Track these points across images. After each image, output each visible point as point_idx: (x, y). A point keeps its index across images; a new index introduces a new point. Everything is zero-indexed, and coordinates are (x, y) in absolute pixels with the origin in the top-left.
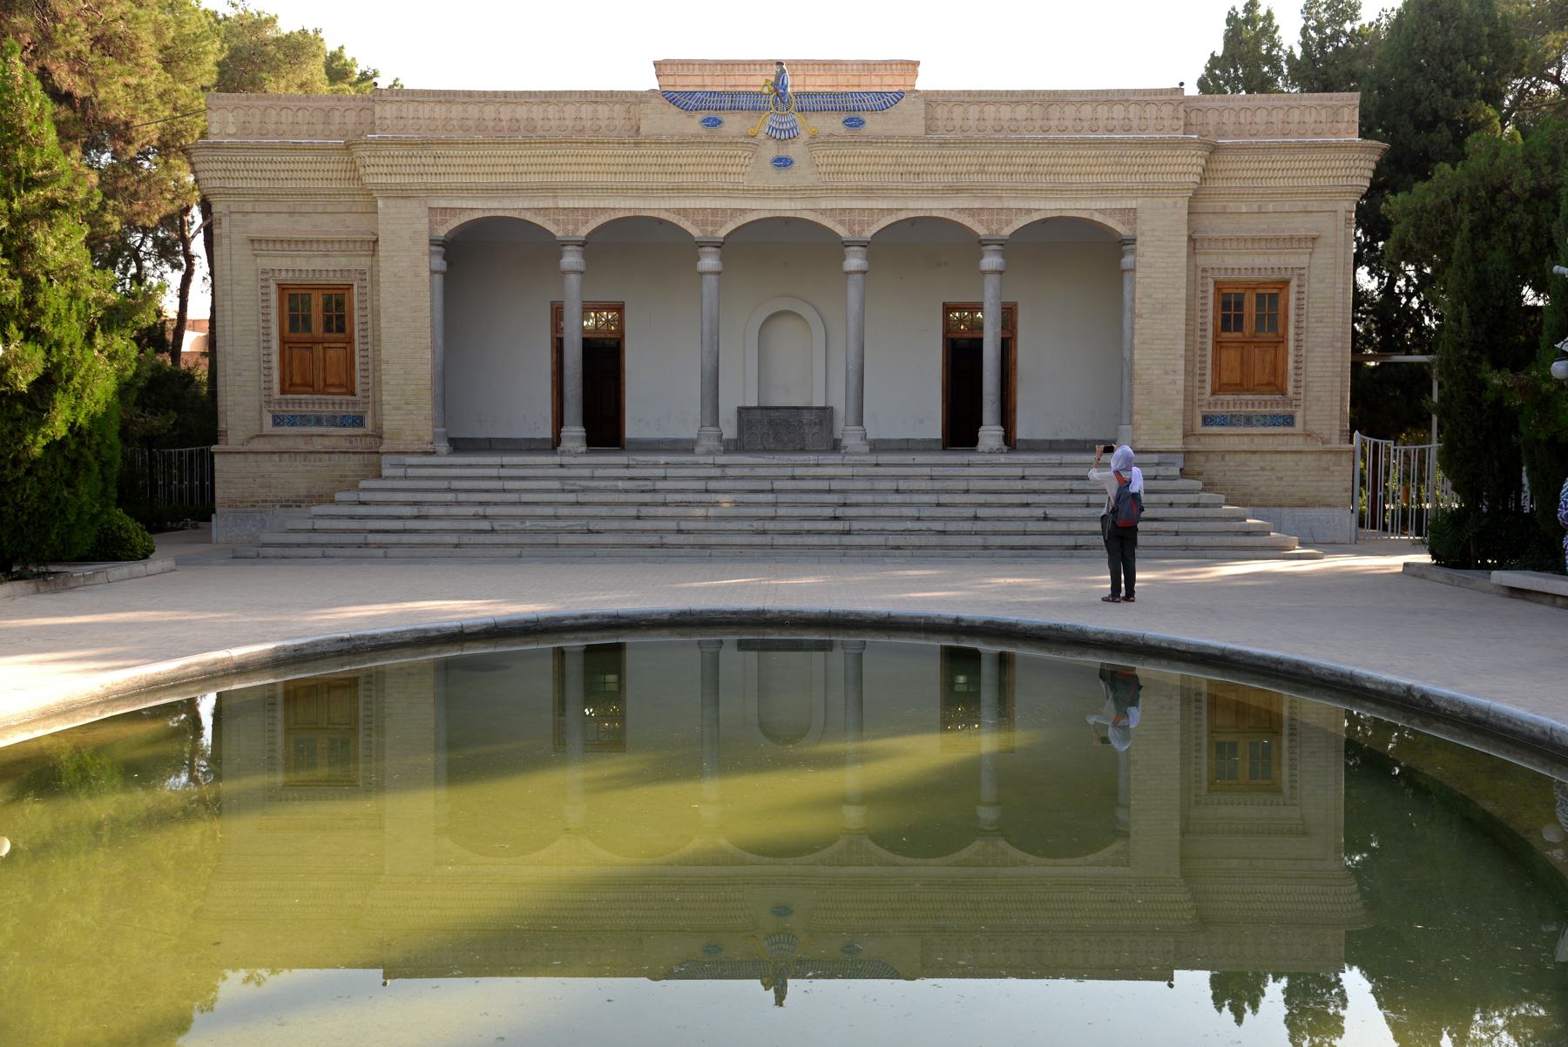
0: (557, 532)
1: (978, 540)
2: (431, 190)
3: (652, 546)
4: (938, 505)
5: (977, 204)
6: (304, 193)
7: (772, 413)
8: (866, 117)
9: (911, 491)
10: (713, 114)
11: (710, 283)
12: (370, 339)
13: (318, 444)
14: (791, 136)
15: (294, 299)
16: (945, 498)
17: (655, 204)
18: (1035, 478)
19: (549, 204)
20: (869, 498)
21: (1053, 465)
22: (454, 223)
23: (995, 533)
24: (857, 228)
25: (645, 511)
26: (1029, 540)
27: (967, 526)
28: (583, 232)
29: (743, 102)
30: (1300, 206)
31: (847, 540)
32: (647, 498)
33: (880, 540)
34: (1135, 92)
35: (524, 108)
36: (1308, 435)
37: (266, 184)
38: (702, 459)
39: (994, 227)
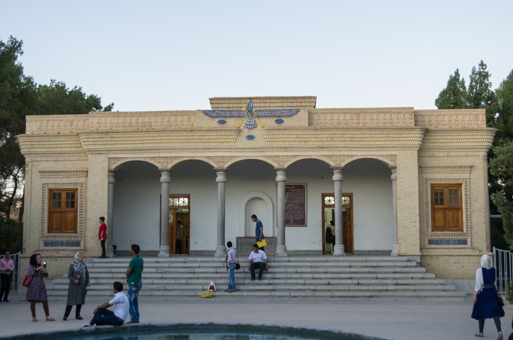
0: (152, 290)
1: (329, 294)
2: (109, 151)
3: (192, 296)
4: (314, 278)
5: (331, 153)
6: (60, 153)
7: (250, 240)
8: (284, 119)
9: (302, 273)
10: (223, 119)
11: (220, 186)
12: (84, 210)
13: (61, 254)
14: (254, 126)
15: (54, 195)
16: (316, 276)
17: (199, 155)
18: (355, 267)
19: (156, 155)
20: (284, 276)
21: (363, 261)
22: (119, 163)
23: (337, 290)
24: (281, 163)
25: (190, 281)
26: (350, 294)
27: (325, 287)
28: (170, 166)
29: (235, 113)
30: (464, 154)
31: (273, 293)
32: (191, 275)
33: (287, 294)
34: (394, 108)
35: (148, 118)
36: (473, 248)
37: (46, 150)
38: (215, 259)
39: (338, 162)
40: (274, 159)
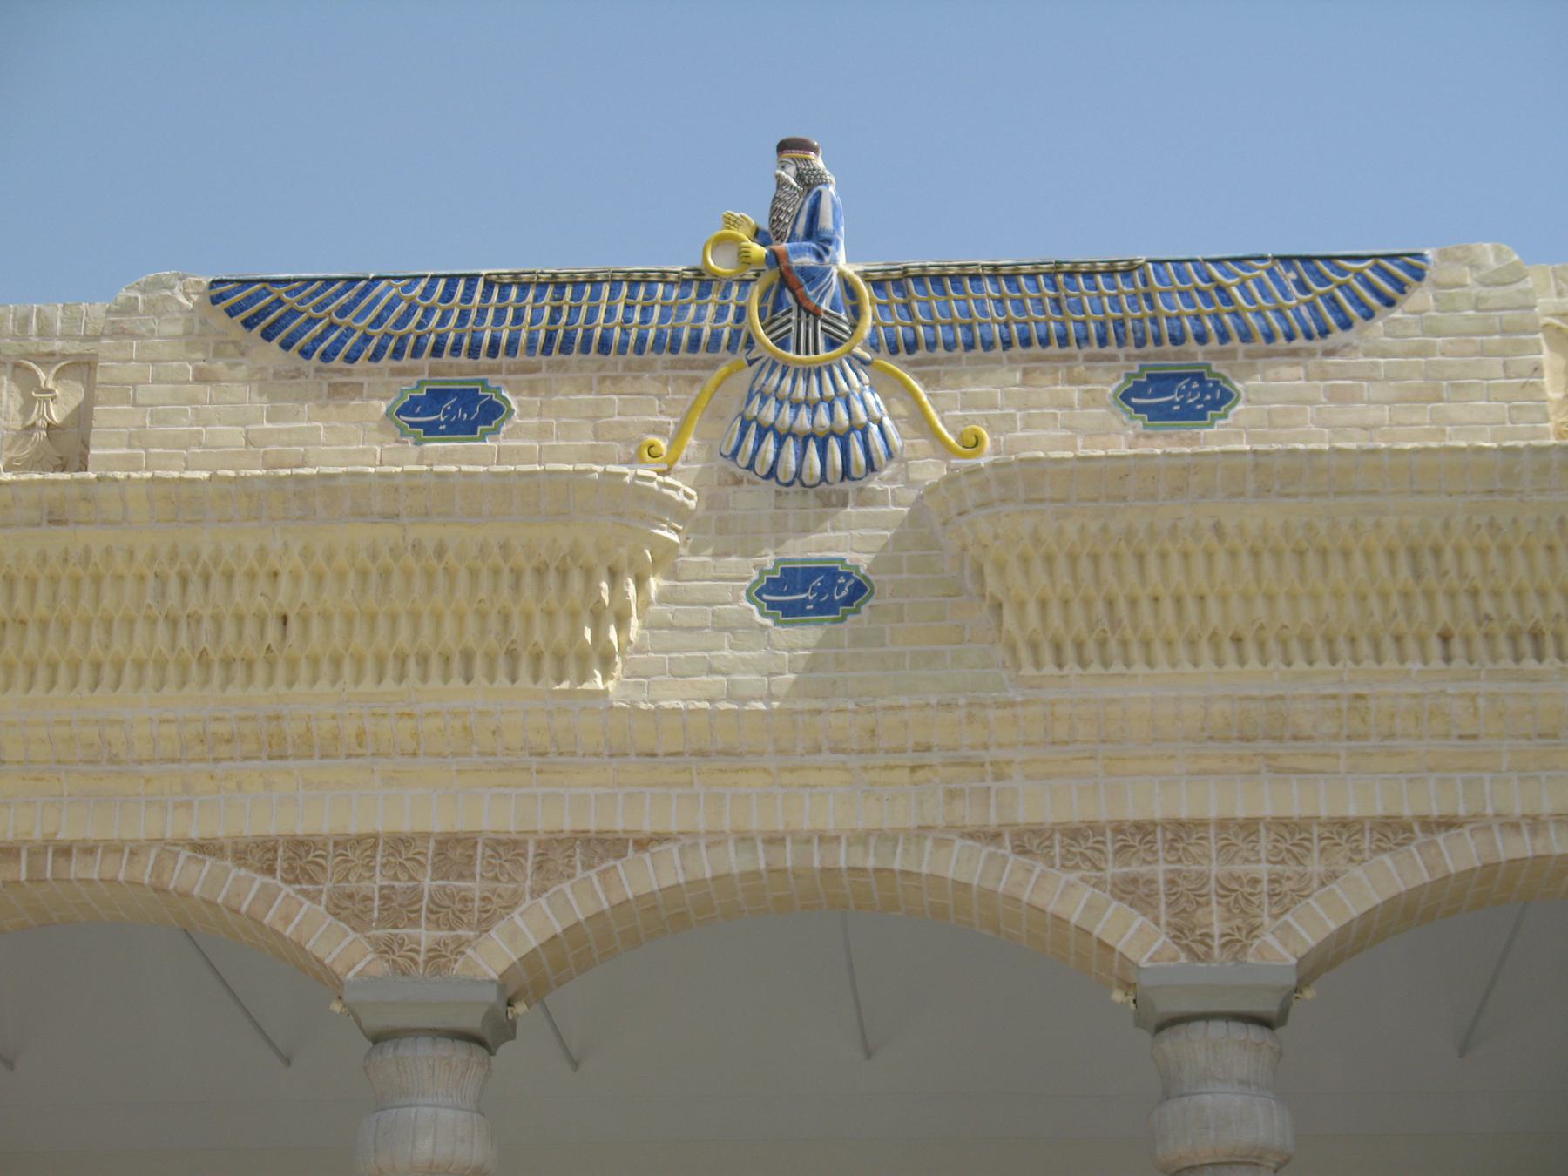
10: (457, 371)
24: (1215, 920)
29: (609, 314)
40: (1112, 870)
